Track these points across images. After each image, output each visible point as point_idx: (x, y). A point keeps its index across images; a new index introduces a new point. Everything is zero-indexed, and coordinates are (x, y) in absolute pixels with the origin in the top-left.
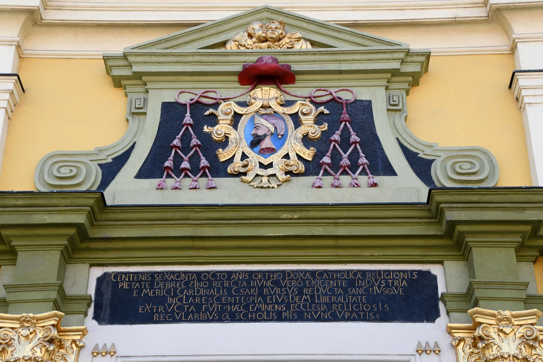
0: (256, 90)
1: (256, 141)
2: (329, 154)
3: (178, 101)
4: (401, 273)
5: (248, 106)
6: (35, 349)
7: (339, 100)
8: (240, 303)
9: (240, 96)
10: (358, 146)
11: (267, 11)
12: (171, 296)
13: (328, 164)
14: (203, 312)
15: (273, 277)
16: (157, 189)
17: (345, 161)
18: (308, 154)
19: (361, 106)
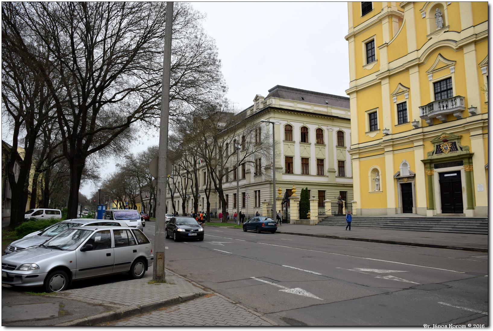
1: (445, 149)
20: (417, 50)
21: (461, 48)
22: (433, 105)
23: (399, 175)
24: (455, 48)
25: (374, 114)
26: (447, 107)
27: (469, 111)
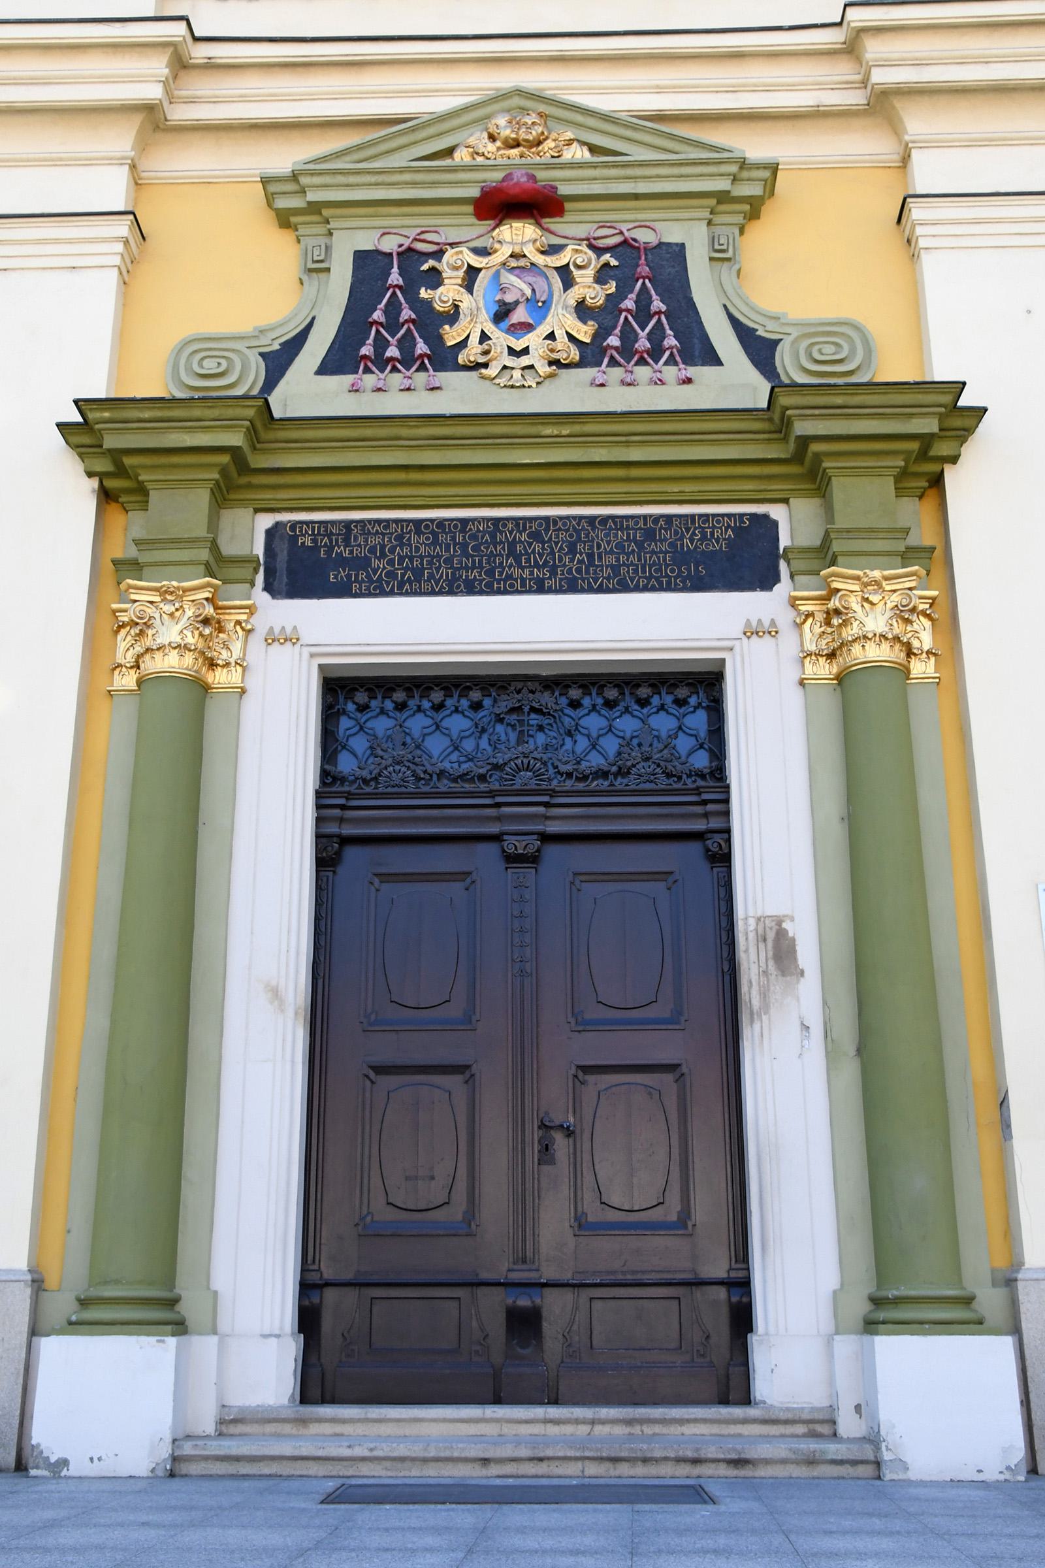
0: (502, 228)
1: (502, 314)
2: (617, 331)
3: (380, 248)
4: (726, 519)
5: (490, 254)
6: (185, 632)
7: (633, 243)
8: (481, 567)
9: (477, 238)
10: (663, 317)
11: (519, 94)
12: (376, 557)
13: (616, 349)
14: (425, 581)
15: (531, 527)
16: (350, 391)
17: (643, 344)
18: (584, 333)
19: (668, 253)
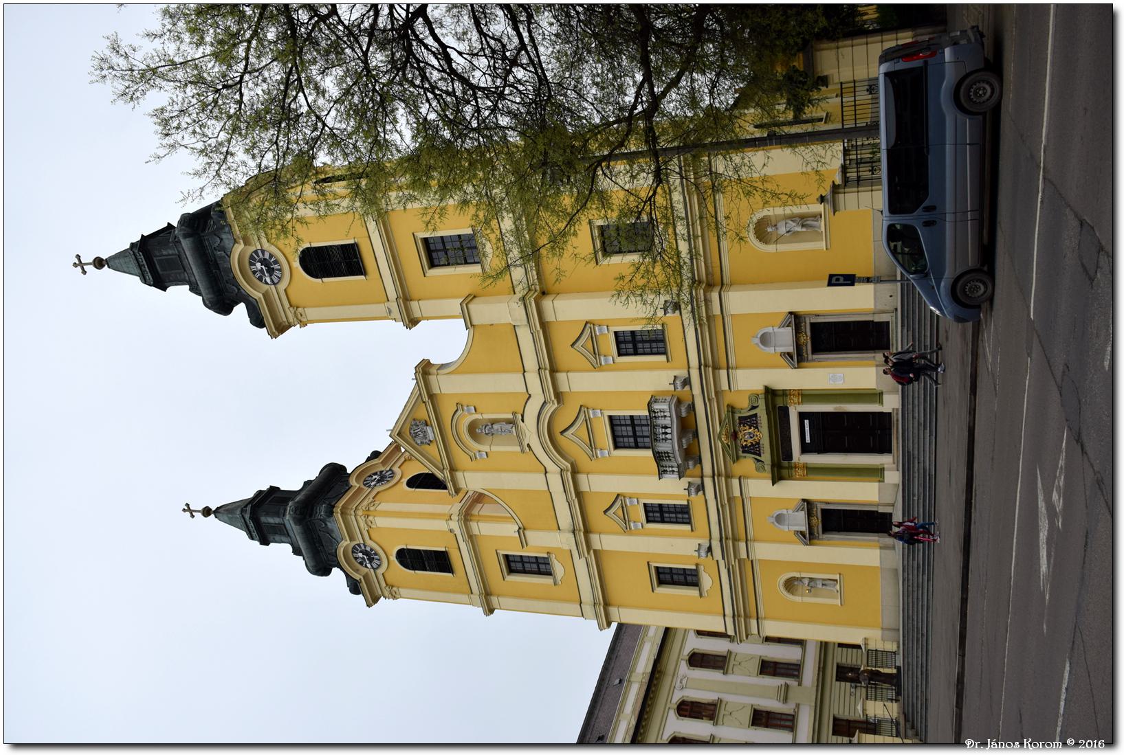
1: (751, 438)
20: (544, 472)
21: (559, 396)
22: (658, 452)
23: (802, 533)
24: (556, 405)
25: (661, 573)
26: (666, 427)
27: (679, 388)
